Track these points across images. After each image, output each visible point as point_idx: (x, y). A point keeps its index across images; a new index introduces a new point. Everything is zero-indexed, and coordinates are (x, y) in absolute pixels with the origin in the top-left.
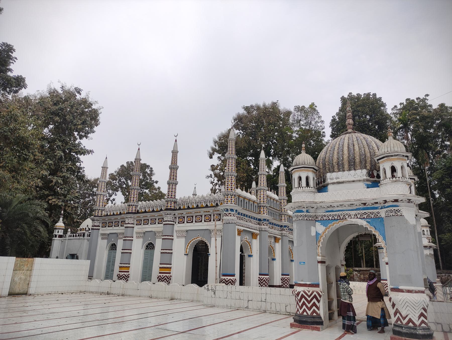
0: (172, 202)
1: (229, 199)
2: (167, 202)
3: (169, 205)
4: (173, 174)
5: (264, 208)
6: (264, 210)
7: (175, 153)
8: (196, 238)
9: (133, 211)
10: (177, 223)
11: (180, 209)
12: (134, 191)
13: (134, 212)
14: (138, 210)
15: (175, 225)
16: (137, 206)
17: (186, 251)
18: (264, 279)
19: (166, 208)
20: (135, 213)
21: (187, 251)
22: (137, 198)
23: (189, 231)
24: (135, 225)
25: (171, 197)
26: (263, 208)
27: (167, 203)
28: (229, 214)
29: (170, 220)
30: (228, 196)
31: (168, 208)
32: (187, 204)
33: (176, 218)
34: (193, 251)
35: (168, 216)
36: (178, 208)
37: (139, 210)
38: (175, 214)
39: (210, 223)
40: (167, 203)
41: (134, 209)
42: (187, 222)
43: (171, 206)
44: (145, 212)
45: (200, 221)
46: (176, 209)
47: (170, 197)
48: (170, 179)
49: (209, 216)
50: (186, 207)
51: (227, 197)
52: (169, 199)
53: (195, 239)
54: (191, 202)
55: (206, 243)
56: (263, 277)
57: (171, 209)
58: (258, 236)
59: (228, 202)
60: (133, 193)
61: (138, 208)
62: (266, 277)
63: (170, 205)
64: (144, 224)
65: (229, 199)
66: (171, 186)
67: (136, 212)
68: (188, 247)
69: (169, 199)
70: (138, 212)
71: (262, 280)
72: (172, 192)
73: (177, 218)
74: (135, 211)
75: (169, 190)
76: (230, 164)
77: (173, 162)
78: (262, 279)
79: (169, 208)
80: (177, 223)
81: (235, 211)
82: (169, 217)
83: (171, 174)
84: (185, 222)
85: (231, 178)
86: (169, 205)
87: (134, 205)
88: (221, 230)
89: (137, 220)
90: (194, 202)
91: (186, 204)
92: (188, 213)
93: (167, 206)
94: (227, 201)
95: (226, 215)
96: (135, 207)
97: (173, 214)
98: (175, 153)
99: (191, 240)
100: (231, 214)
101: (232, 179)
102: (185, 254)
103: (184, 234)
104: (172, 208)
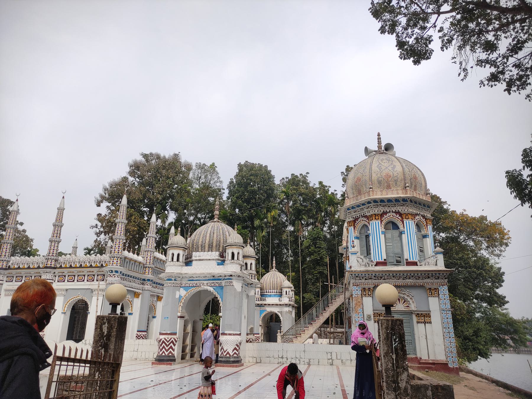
0: (53, 260)
1: (115, 261)
2: (47, 260)
3: (49, 263)
4: (57, 231)
5: (149, 269)
6: (149, 271)
7: (61, 211)
8: (77, 297)
9: (4, 267)
10: (56, 281)
11: (61, 267)
12: (7, 245)
13: (5, 267)
14: (9, 266)
15: (54, 283)
16: (9, 261)
17: (64, 310)
18: (142, 335)
19: (45, 266)
20: (5, 269)
21: (65, 310)
22: (9, 253)
23: (69, 290)
24: (4, 282)
25: (52, 255)
26: (148, 268)
27: (48, 261)
28: (114, 275)
29: (49, 278)
30: (114, 259)
31: (48, 266)
32: (69, 263)
33: (55, 276)
34: (71, 310)
35: (47, 274)
36: (58, 266)
37: (11, 265)
38: (54, 273)
39: (93, 283)
40: (48, 261)
41: (5, 264)
42: (68, 281)
43: (51, 265)
44: (19, 268)
45: (82, 280)
46: (56, 267)
47: (51, 255)
48: (53, 236)
49: (92, 276)
50: (68, 266)
51: (113, 260)
52: (50, 257)
53: (72, 300)
54: (74, 262)
55: (86, 302)
56: (141, 333)
57: (50, 268)
58: (141, 296)
59: (114, 264)
60: (6, 247)
61: (10, 264)
62: (143, 333)
63: (50, 263)
64: (16, 281)
65: (115, 261)
66: (53, 244)
67: (7, 268)
68: (67, 306)
69: (50, 257)
70: (9, 268)
71: (139, 336)
72: (54, 250)
73: (57, 277)
74: (6, 266)
75: (50, 247)
76: (119, 228)
77: (58, 219)
78: (139, 335)
79: (49, 266)
80: (56, 281)
81: (119, 273)
82: (48, 276)
83: (54, 232)
84: (66, 281)
85: (119, 242)
86: (49, 263)
87: (5, 260)
88: (104, 290)
89: (7, 277)
90: (78, 262)
91: (68, 262)
92: (70, 272)
93: (47, 264)
94: (113, 263)
95: (110, 276)
96: (6, 262)
97: (53, 272)
98: (61, 211)
99: (68, 301)
100: (115, 275)
101: (119, 243)
102: (62, 313)
103: (63, 293)
104: (52, 266)
